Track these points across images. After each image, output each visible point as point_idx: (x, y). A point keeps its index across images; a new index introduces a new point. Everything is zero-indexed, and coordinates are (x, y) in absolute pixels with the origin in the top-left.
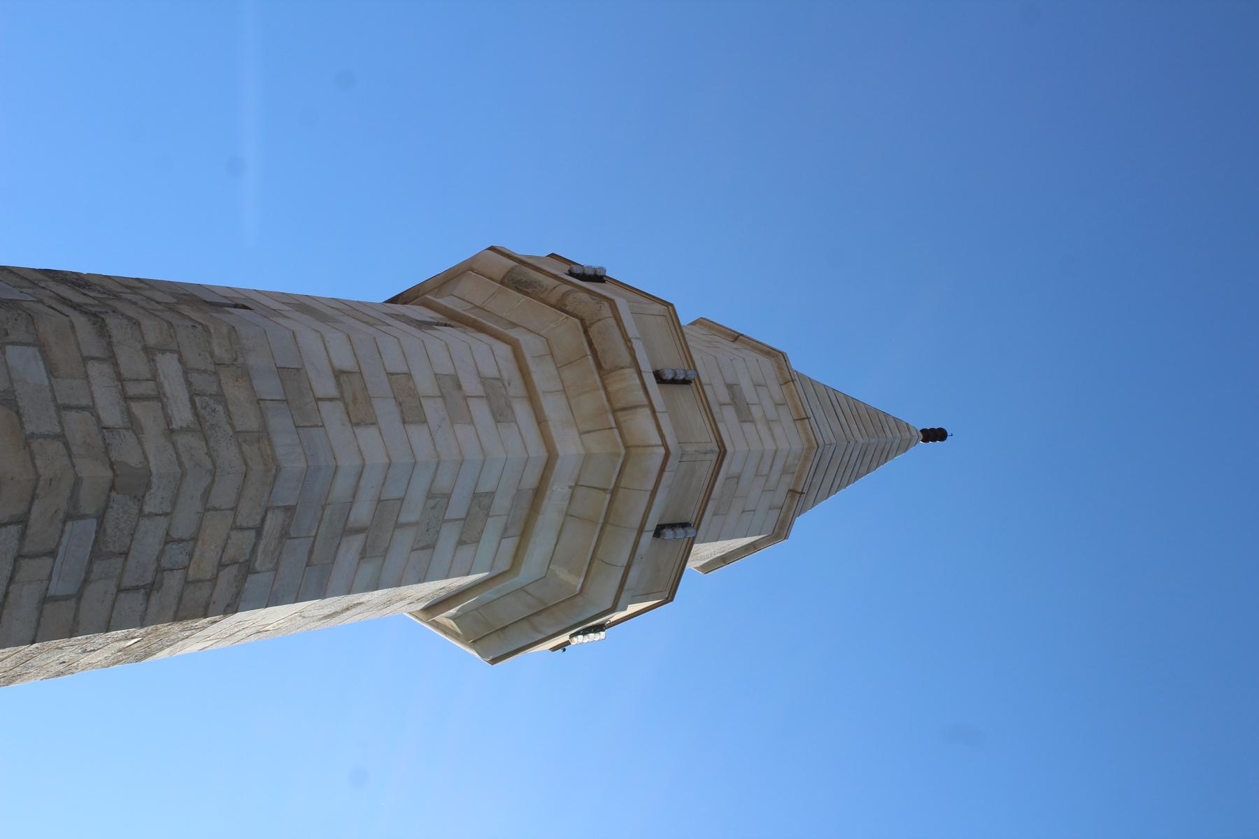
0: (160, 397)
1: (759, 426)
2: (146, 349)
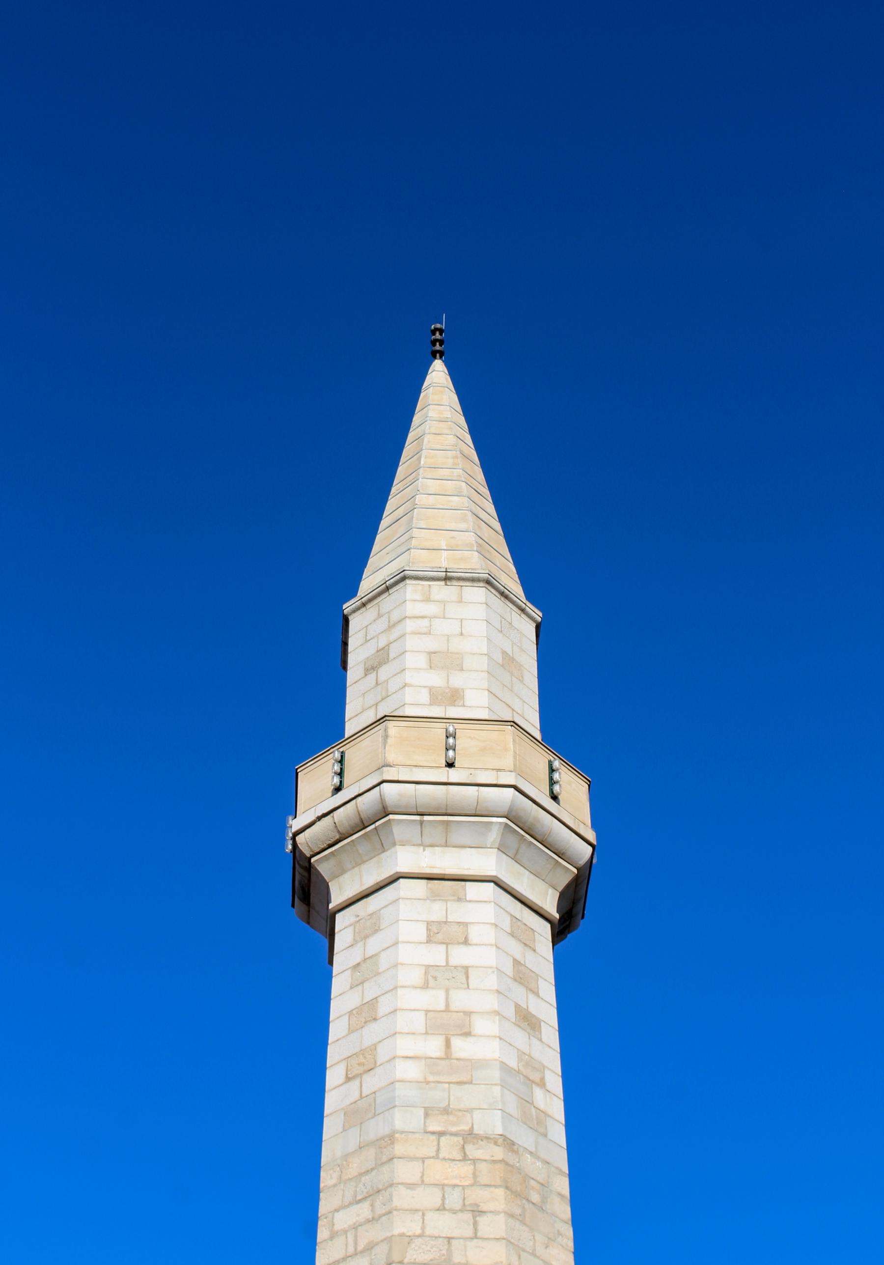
0: (355, 1227)
1: (392, 638)
2: (331, 1238)
